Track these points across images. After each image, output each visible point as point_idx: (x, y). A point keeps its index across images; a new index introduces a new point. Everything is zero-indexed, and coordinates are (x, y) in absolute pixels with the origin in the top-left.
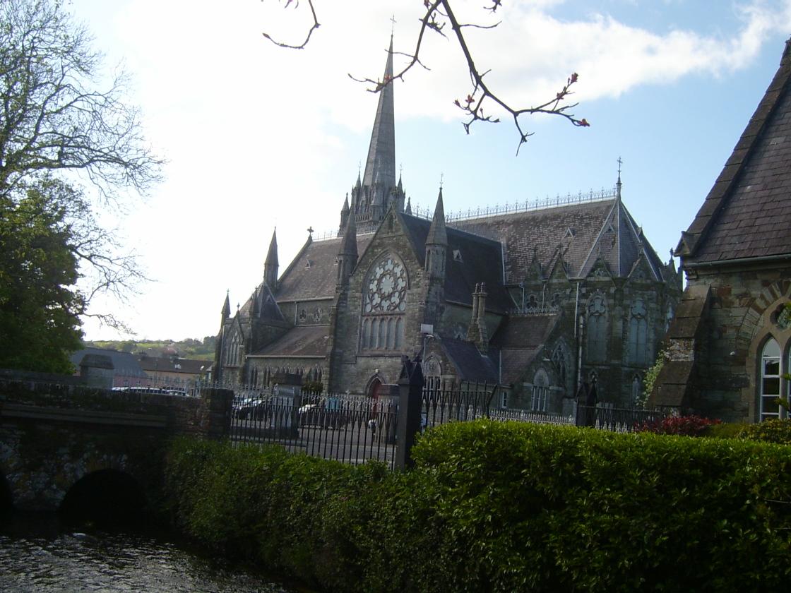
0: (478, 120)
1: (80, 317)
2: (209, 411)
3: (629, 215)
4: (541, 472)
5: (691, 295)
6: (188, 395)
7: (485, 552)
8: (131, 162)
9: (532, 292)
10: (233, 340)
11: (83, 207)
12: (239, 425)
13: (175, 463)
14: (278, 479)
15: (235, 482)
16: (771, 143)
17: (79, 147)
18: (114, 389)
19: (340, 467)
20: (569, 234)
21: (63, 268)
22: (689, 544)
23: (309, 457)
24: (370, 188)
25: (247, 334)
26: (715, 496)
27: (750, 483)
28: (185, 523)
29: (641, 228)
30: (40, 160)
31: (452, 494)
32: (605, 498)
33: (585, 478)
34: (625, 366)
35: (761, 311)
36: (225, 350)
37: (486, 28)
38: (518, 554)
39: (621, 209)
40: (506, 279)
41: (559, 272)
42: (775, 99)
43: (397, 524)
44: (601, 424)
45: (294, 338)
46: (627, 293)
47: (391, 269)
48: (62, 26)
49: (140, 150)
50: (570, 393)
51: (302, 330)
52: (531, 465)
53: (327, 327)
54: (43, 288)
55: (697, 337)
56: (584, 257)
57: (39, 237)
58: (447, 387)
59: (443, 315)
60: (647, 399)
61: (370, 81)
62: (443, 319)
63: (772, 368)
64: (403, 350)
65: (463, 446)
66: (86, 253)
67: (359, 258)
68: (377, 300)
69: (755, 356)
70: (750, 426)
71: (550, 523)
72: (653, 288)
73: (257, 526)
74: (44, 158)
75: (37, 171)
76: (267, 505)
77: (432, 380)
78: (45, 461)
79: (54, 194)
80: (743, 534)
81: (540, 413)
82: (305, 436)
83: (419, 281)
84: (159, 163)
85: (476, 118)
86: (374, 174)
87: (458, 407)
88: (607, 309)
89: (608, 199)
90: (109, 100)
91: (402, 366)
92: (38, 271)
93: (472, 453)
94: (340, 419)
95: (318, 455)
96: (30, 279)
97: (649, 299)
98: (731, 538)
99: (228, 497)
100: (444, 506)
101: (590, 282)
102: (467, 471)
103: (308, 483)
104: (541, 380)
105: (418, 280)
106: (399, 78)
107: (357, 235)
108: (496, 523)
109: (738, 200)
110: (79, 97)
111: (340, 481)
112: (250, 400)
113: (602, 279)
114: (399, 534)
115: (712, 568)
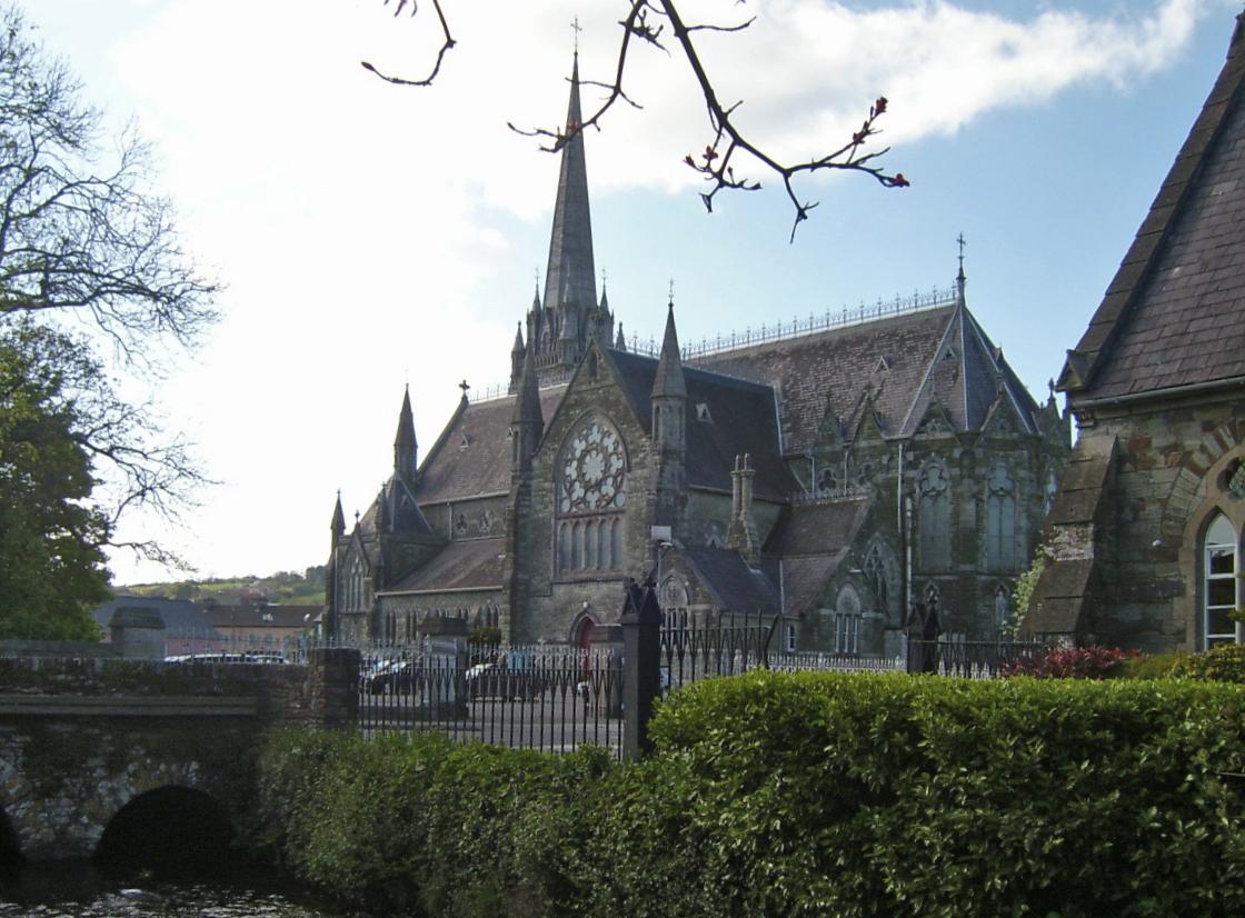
0: (726, 188)
1: (104, 548)
2: (323, 684)
3: (977, 324)
4: (856, 748)
5: (1085, 453)
6: (287, 662)
7: (773, 878)
8: (163, 291)
9: (827, 464)
10: (353, 571)
11: (91, 370)
12: (373, 704)
13: (275, 769)
14: (441, 785)
15: (372, 793)
16: (1214, 193)
17: (74, 271)
18: (167, 659)
19: (537, 759)
20: (882, 367)
21: (67, 471)
22: (1097, 849)
23: (487, 748)
24: (556, 311)
25: (374, 559)
26: (1137, 770)
27: (1191, 748)
28: (298, 862)
29: (1000, 349)
30: (11, 296)
31: (715, 790)
32: (960, 783)
33: (925, 754)
34: (982, 574)
35: (1201, 472)
36: (341, 586)
37: (731, 30)
38: (826, 877)
39: (965, 319)
40: (783, 444)
41: (869, 428)
42: (1219, 118)
43: (632, 843)
44: (948, 667)
45: (450, 560)
46: (981, 455)
47: (598, 441)
48: (24, 67)
49: (176, 270)
50: (896, 621)
51: (464, 546)
52: (839, 738)
53: (502, 539)
54: (38, 505)
55: (1097, 520)
56: (909, 403)
57: (21, 423)
58: (698, 623)
59: (687, 509)
60: (1019, 624)
61: (544, 132)
62: (686, 516)
63: (1222, 563)
64: (625, 569)
65: (730, 714)
66: (103, 445)
67: (546, 426)
68: (579, 492)
69: (1194, 546)
70: (1189, 657)
71: (874, 826)
72: (1024, 446)
73: (412, 859)
74: (17, 292)
75: (9, 315)
76: (426, 826)
77: (675, 614)
78: (67, 781)
79: (40, 351)
80: (1183, 828)
81: (848, 656)
82: (479, 714)
83: (644, 458)
84: (209, 290)
85: (722, 184)
86: (561, 289)
87: (718, 654)
88: (950, 484)
89: (944, 304)
90: (117, 190)
91: (625, 594)
92: (27, 479)
93: (744, 724)
94: (531, 684)
95: (502, 743)
96: (15, 492)
97: (1017, 464)
98: (1164, 835)
99: (364, 817)
100: (704, 809)
101: (922, 441)
102: (738, 753)
103: (488, 788)
104: (847, 603)
105: (642, 455)
106: (592, 125)
107: (540, 389)
108: (788, 831)
109: (1161, 292)
110: (66, 188)
111: (538, 780)
112: (387, 663)
113: (939, 436)
114: (635, 858)
115: (1135, 884)
